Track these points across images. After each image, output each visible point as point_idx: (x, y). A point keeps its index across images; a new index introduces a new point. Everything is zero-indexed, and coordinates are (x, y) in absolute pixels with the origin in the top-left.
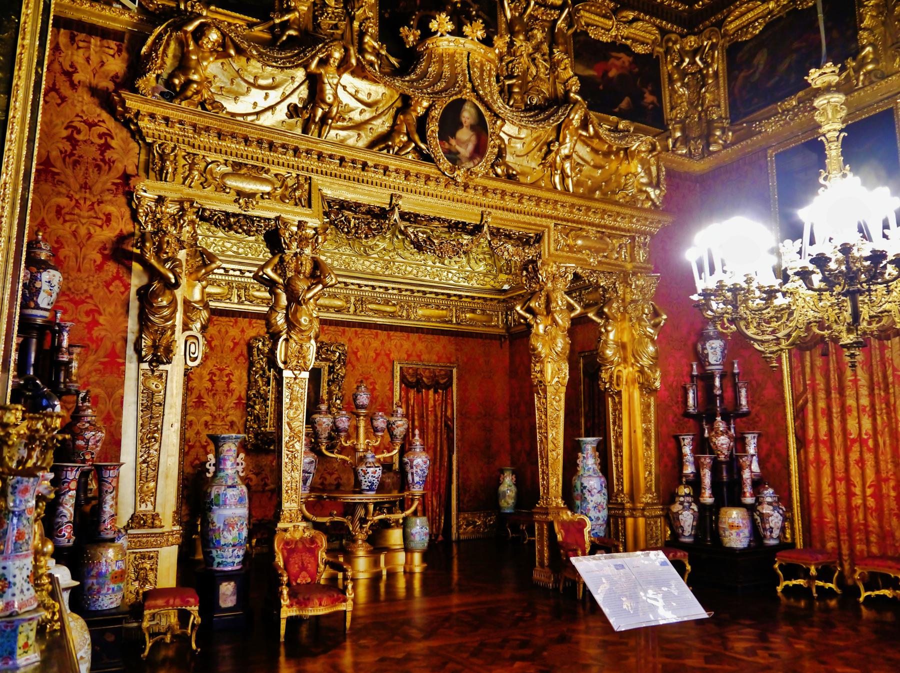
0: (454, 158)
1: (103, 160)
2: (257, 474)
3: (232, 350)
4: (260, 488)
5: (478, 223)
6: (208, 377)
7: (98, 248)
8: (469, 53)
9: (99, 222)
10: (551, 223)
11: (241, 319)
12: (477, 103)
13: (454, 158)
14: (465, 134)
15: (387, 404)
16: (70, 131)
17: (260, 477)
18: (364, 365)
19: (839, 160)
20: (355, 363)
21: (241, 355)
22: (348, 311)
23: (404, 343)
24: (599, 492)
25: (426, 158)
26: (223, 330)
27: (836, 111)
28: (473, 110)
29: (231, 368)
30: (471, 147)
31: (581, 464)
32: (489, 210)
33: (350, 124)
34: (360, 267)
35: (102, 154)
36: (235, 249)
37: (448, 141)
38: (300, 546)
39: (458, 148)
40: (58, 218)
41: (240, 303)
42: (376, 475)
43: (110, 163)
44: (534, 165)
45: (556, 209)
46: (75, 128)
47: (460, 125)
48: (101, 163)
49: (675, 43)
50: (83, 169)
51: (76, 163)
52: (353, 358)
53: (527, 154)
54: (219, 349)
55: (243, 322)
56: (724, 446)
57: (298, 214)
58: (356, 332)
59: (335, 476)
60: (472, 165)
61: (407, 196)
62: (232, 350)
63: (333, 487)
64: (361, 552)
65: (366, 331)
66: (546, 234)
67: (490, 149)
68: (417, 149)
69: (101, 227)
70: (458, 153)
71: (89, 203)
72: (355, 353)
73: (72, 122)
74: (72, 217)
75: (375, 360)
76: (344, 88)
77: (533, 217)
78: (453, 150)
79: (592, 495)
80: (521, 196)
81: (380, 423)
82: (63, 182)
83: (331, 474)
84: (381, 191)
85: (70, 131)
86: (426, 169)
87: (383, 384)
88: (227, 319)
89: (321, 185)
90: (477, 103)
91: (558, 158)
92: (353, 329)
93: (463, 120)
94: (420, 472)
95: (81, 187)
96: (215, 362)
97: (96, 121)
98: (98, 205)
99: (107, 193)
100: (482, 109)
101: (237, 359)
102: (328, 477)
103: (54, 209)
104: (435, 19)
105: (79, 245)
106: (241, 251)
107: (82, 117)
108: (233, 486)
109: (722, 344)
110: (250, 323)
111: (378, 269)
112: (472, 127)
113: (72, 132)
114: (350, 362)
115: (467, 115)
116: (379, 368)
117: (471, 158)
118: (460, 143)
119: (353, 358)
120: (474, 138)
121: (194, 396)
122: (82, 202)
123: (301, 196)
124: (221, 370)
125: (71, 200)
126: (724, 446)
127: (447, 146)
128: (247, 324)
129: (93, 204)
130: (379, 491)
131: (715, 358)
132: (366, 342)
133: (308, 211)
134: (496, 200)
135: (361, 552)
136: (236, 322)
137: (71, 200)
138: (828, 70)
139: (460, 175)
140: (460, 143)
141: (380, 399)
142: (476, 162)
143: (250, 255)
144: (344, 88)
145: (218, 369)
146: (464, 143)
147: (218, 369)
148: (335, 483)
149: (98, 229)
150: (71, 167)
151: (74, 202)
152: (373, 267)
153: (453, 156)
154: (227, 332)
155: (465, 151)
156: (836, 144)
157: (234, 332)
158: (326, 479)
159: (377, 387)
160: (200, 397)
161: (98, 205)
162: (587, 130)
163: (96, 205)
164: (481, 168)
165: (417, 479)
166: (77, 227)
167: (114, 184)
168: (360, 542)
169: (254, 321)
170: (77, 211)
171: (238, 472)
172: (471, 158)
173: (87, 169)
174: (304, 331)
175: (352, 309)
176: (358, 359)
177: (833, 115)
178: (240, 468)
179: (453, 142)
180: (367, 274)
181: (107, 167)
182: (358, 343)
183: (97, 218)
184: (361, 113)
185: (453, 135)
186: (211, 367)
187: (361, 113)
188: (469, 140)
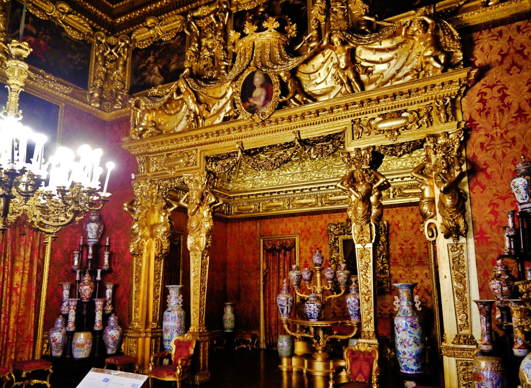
1: (504, 105)
2: (339, 306)
3: (321, 233)
4: (341, 315)
6: (309, 250)
7: (510, 162)
9: (508, 145)
11: (324, 215)
13: (252, 110)
15: (424, 258)
16: (480, 96)
17: (341, 308)
18: (404, 232)
19: (15, 105)
20: (397, 232)
21: (325, 236)
22: (389, 198)
23: (299, 223)
24: (404, 330)
26: (315, 223)
27: (21, 72)
29: (321, 244)
30: (263, 98)
31: (398, 306)
33: (215, 112)
34: (395, 167)
35: (502, 102)
36: (317, 176)
37: (248, 101)
38: (184, 344)
39: (255, 102)
40: (483, 150)
41: (322, 206)
42: (312, 309)
43: (508, 106)
46: (483, 93)
47: (254, 88)
48: (503, 108)
49: (102, 38)
50: (492, 115)
51: (487, 114)
52: (396, 229)
54: (314, 234)
55: (326, 216)
56: (496, 291)
57: (192, 169)
58: (397, 211)
59: (389, 308)
62: (321, 233)
63: (387, 316)
64: (319, 358)
65: (405, 209)
69: (510, 147)
70: (255, 105)
71: (499, 135)
72: (397, 225)
73: (480, 90)
74: (491, 147)
75: (412, 228)
78: (252, 105)
79: (399, 333)
80: (317, 112)
81: (328, 274)
82: (481, 128)
83: (386, 307)
84: (287, 132)
85: (480, 96)
87: (420, 244)
88: (317, 216)
92: (394, 209)
93: (255, 84)
94: (351, 308)
95: (493, 127)
96: (312, 242)
97: (495, 83)
98: (506, 134)
99: (510, 124)
101: (323, 238)
102: (383, 309)
103: (479, 145)
105: (498, 162)
106: (320, 176)
107: (485, 85)
108: (170, 311)
109: (97, 226)
110: (329, 216)
111: (409, 164)
112: (262, 86)
113: (482, 96)
114: (394, 231)
115: (258, 80)
116: (416, 233)
118: (255, 99)
119: (396, 229)
120: (264, 92)
121: (303, 262)
122: (495, 135)
124: (316, 246)
125: (488, 137)
126: (496, 291)
127: (248, 104)
128: (328, 217)
129: (502, 135)
130: (319, 319)
131: (520, 197)
132: (405, 216)
133: (195, 167)
134: (299, 122)
135: (319, 358)
136: (322, 217)
137: (488, 137)
138: (23, 46)
141: (418, 255)
142: (267, 105)
143: (325, 177)
145: (314, 245)
146: (259, 97)
147: (314, 245)
148: (389, 313)
149: (508, 149)
150: (485, 117)
151: (490, 137)
152: (404, 164)
153: (253, 109)
154: (317, 224)
155: (259, 103)
156: (16, 94)
157: (321, 223)
158: (382, 310)
159: (415, 246)
160: (306, 262)
161: (506, 134)
163: (504, 135)
165: (351, 312)
166: (495, 152)
167: (513, 117)
168: (320, 352)
169: (331, 214)
170: (493, 142)
171: (178, 304)
173: (495, 115)
174: (194, 230)
175: (391, 196)
176: (399, 229)
177: (18, 75)
178: (180, 303)
179: (251, 100)
180: (400, 170)
181: (507, 108)
182: (398, 218)
183: (506, 143)
185: (251, 96)
186: (311, 244)
187: (218, 104)
188: (261, 94)
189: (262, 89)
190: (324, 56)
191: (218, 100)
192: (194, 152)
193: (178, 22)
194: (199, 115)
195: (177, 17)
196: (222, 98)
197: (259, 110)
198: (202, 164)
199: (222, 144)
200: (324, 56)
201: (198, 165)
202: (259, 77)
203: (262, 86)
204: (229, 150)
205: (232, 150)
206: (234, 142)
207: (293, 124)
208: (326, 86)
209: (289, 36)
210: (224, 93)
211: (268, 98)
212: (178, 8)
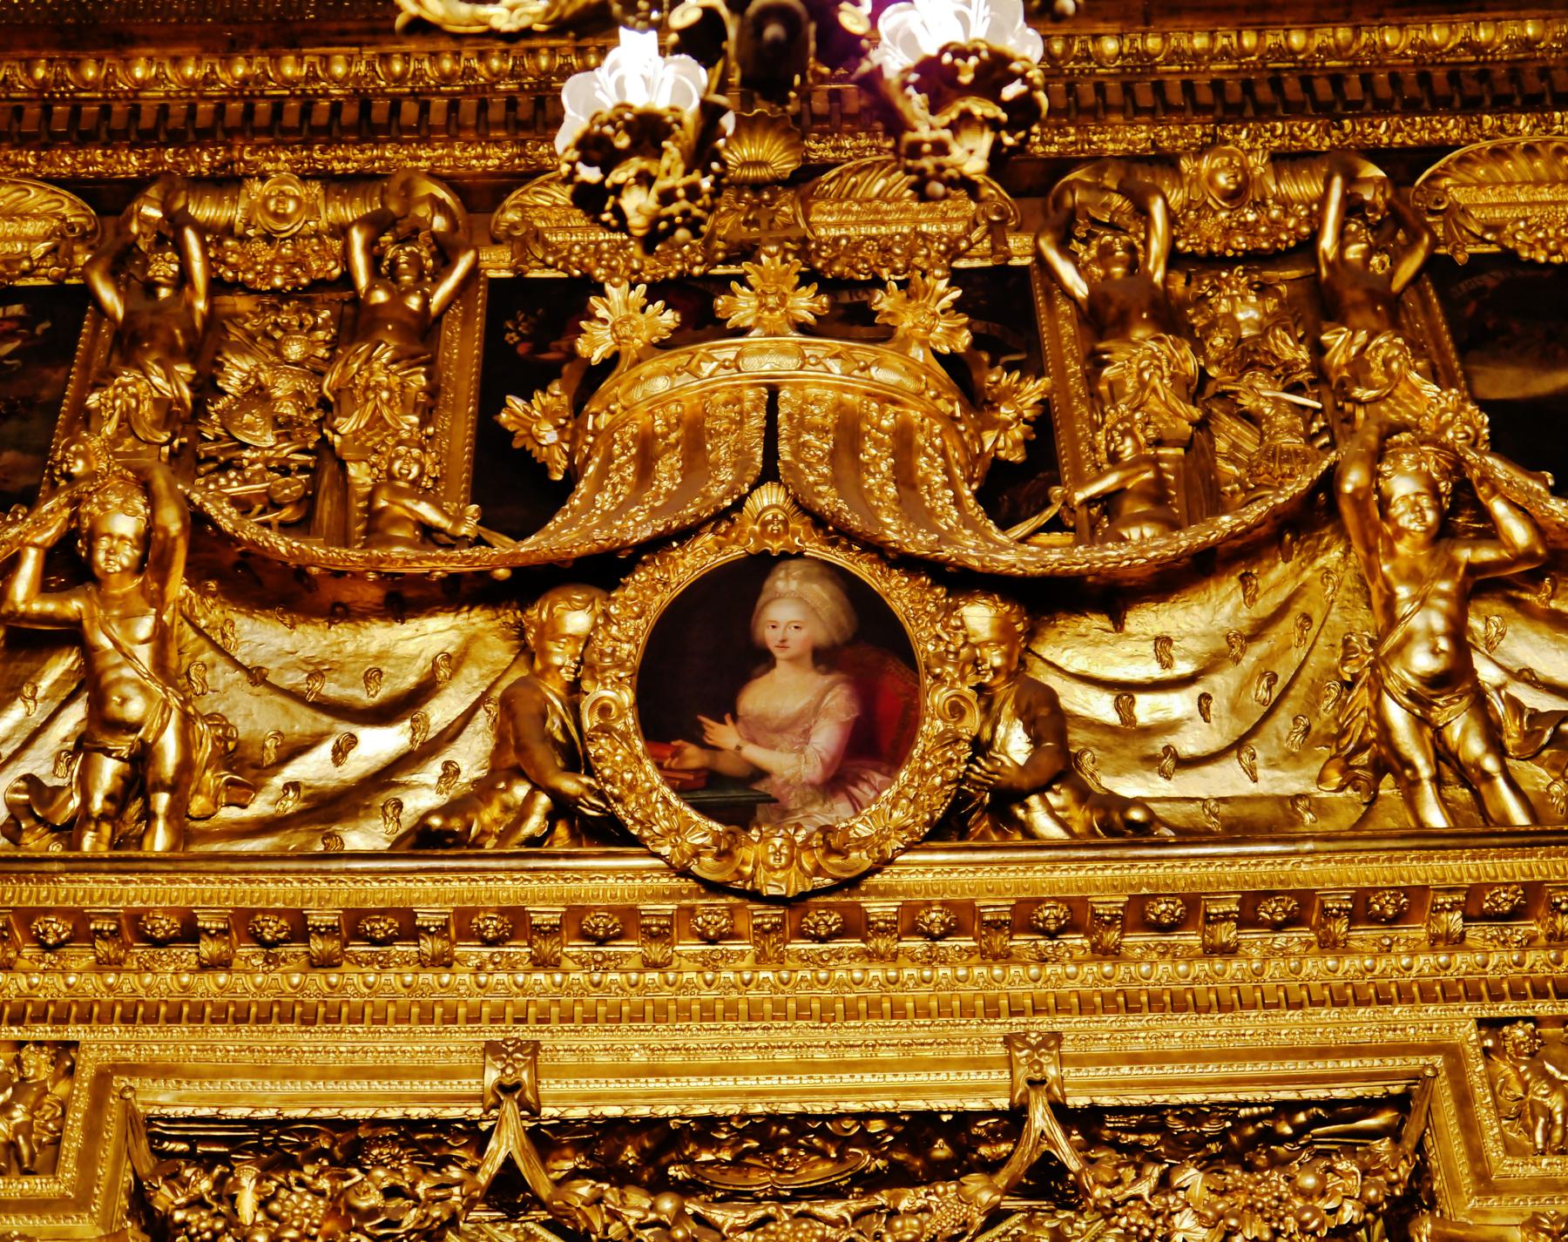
0: (736, 800)
5: (1002, 1103)
8: (774, 391)
10: (1459, 1024)
12: (838, 558)
13: (736, 800)
14: (781, 692)
25: (608, 833)
28: (820, 593)
30: (826, 738)
32: (1044, 1024)
33: (291, 805)
44: (1291, 782)
45: (1457, 942)
47: (763, 659)
53: (1238, 745)
60: (842, 808)
61: (563, 1041)
66: (1444, 1092)
67: (932, 726)
68: (563, 808)
70: (760, 774)
76: (256, 676)
77: (1327, 1014)
78: (726, 765)
86: (606, 879)
89: (133, 1070)
90: (838, 558)
91: (1397, 716)
93: (771, 637)
100: (863, 569)
104: (591, 317)
112: (823, 658)
115: (792, 613)
117: (838, 780)
118: (764, 731)
123: (17, 1130)
127: (693, 756)
134: (1074, 969)
139: (770, 860)
140: (764, 731)
142: (863, 791)
144: (256, 676)
146: (798, 728)
162: (1490, 532)
164: (888, 808)
172: (838, 780)
179: (725, 735)
184: (339, 754)
185: (726, 708)
187: (339, 754)
189: (824, 681)
190: (1251, 600)
191: (344, 728)
192: (38, 1065)
193: (31, 228)
194: (171, 789)
195: (36, 198)
196: (383, 715)
197: (786, 813)
198: (103, 1171)
199: (343, 1044)
200: (1251, 600)
201: (69, 1168)
202: (800, 599)
203: (823, 658)
204: (398, 1098)
205: (424, 1099)
206: (460, 1041)
207: (1017, 980)
208: (1247, 788)
209: (989, 438)
210: (410, 680)
211: (875, 743)
212: (84, 139)
